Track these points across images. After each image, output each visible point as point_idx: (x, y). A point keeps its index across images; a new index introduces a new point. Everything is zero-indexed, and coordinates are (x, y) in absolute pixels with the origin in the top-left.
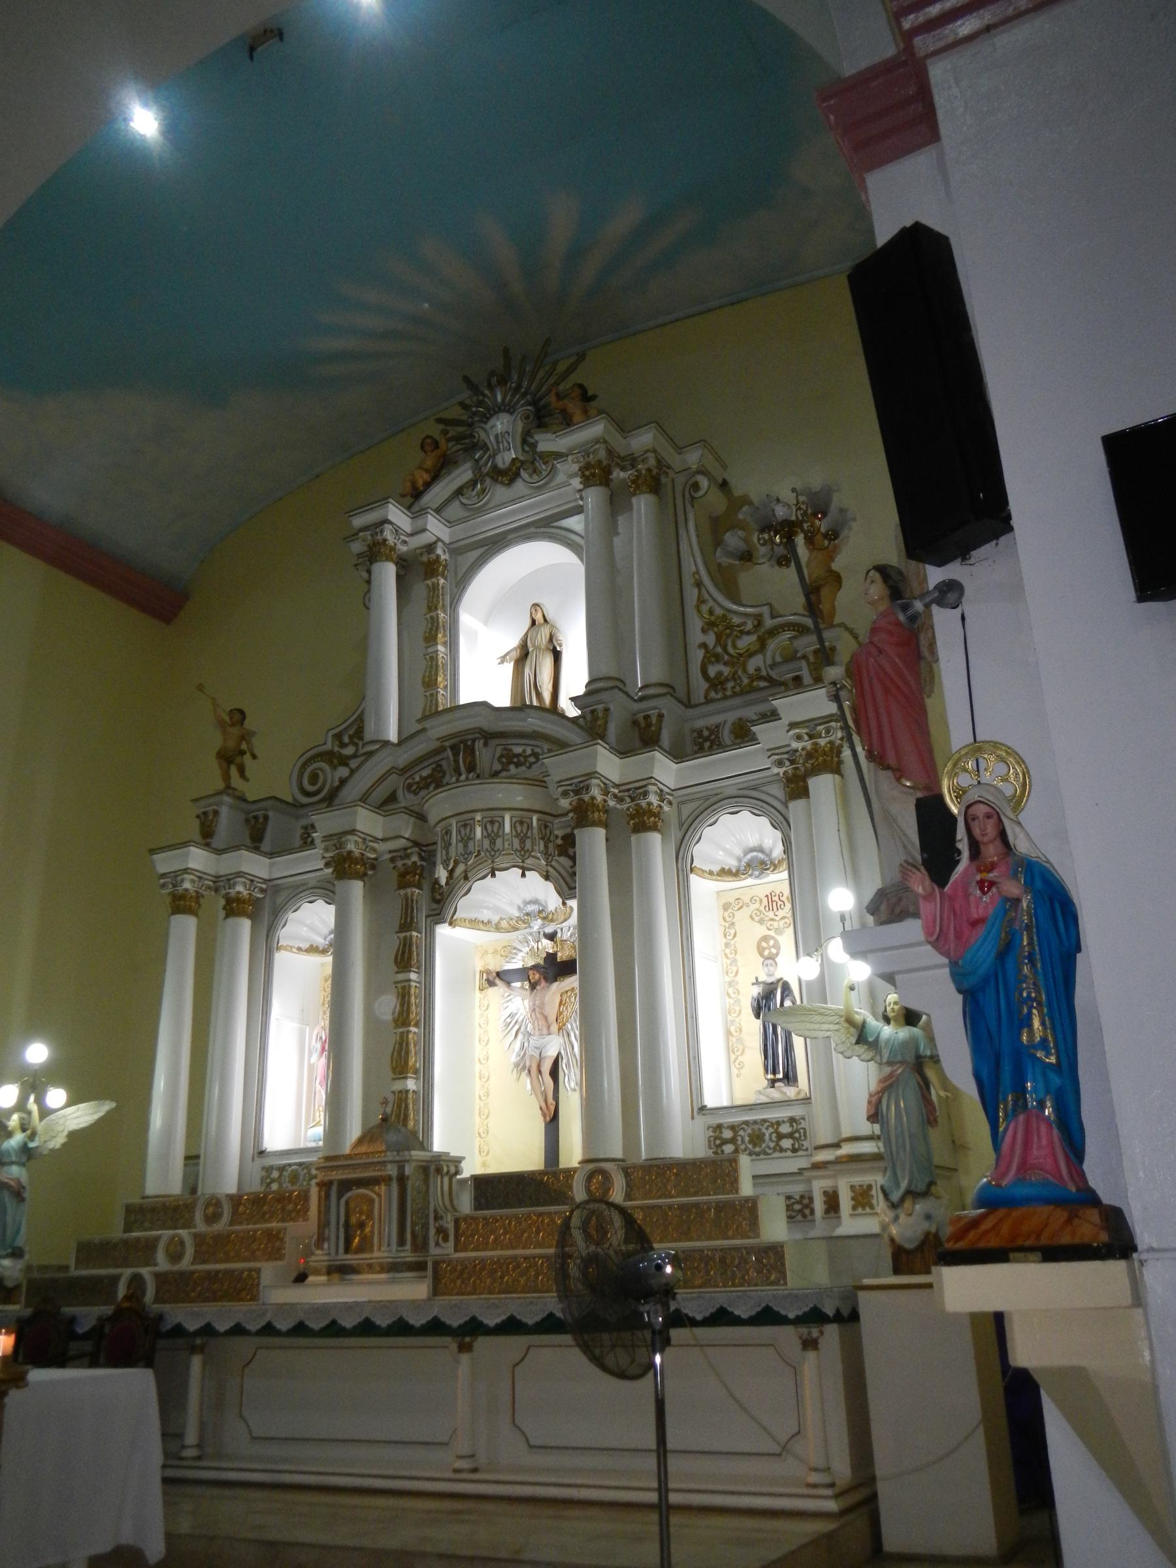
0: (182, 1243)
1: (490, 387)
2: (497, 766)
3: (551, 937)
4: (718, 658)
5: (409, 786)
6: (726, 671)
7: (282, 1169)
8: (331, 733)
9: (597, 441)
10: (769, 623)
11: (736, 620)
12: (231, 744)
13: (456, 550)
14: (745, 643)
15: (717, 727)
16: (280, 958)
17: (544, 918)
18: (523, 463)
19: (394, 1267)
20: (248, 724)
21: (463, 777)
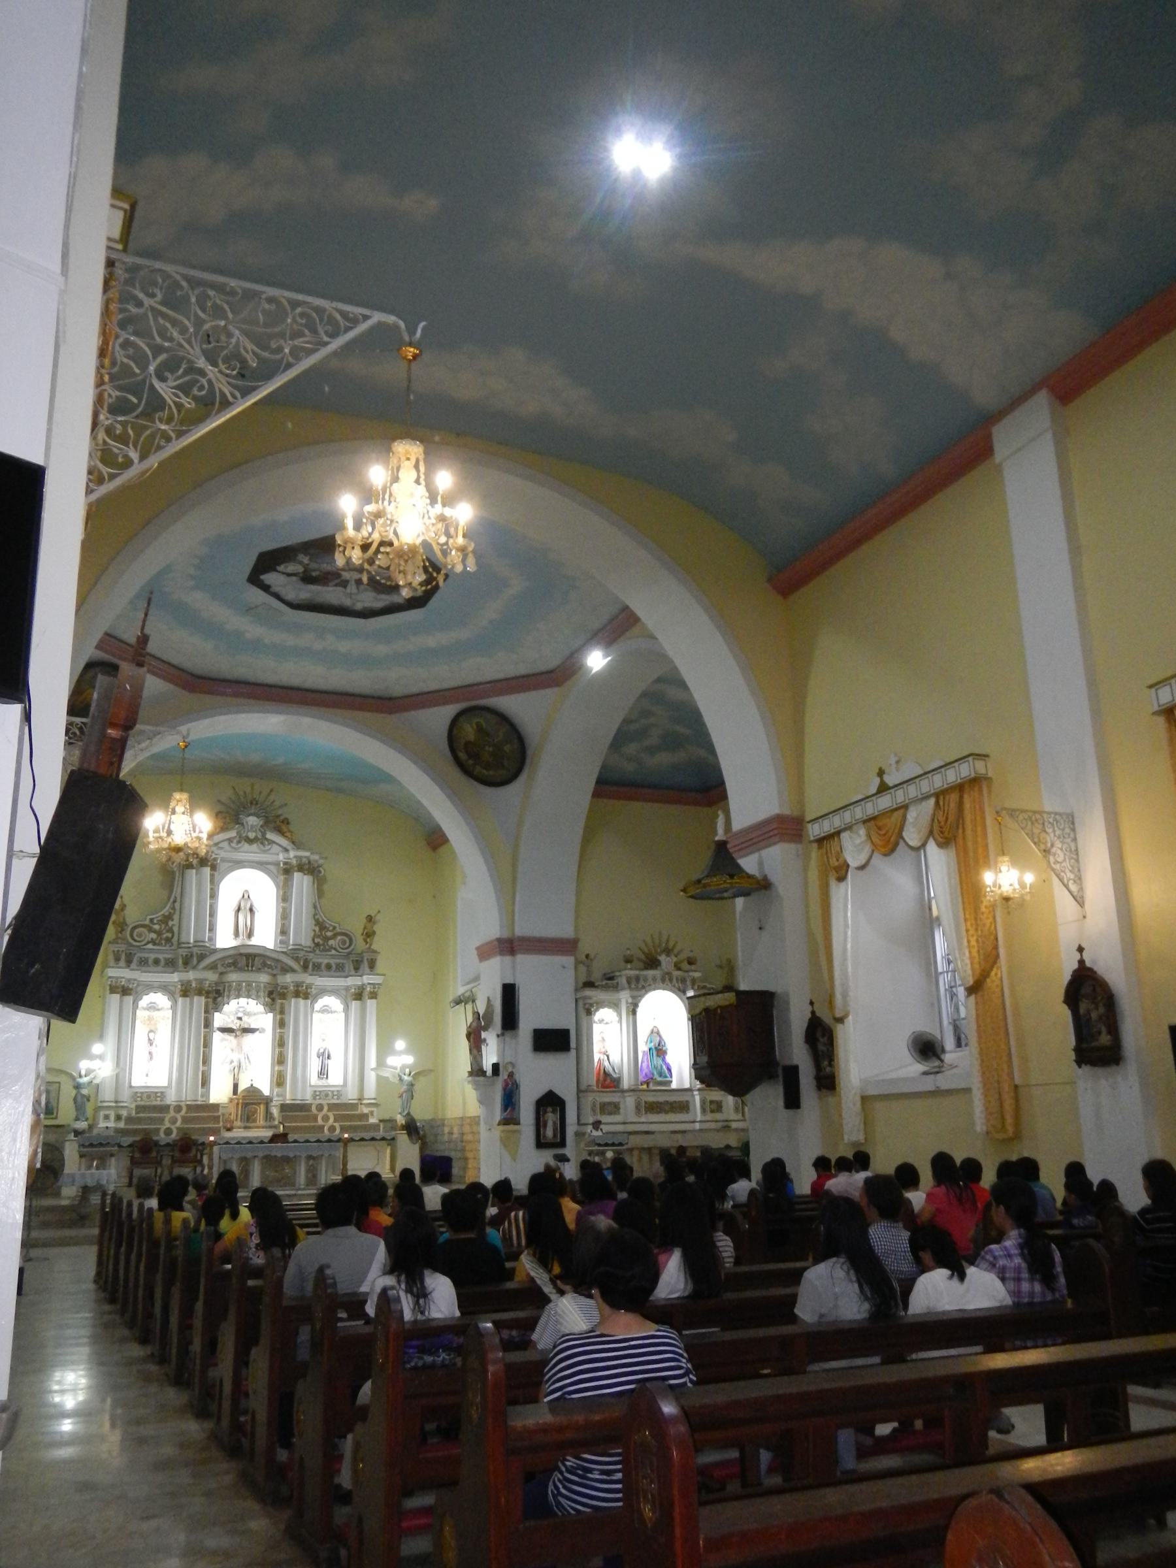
0: (176, 1119)
1: (251, 803)
2: (260, 966)
3: (240, 1019)
4: (318, 937)
5: (223, 965)
6: (321, 942)
7: (142, 1093)
8: (149, 917)
9: (306, 857)
10: (338, 930)
11: (328, 926)
12: (121, 920)
13: (223, 860)
14: (329, 934)
15: (321, 963)
16: (138, 1012)
17: (245, 1014)
18: (259, 839)
19: (263, 1127)
20: (125, 912)
21: (250, 968)
